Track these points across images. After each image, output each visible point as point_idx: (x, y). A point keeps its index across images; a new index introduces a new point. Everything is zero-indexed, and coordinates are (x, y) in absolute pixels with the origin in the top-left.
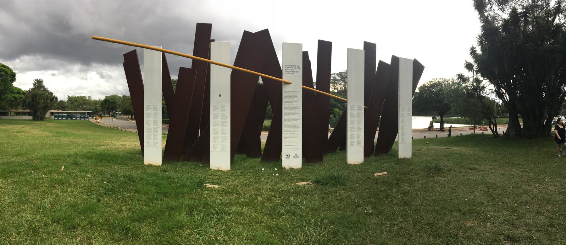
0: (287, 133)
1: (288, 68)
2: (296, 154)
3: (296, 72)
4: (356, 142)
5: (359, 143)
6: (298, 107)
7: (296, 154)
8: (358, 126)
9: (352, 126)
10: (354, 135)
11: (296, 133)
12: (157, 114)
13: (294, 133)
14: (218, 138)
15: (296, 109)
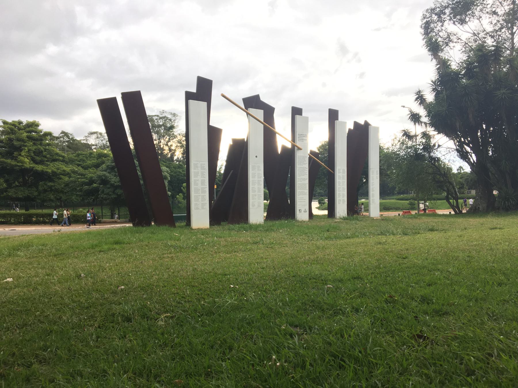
0: (300, 191)
13: (304, 191)
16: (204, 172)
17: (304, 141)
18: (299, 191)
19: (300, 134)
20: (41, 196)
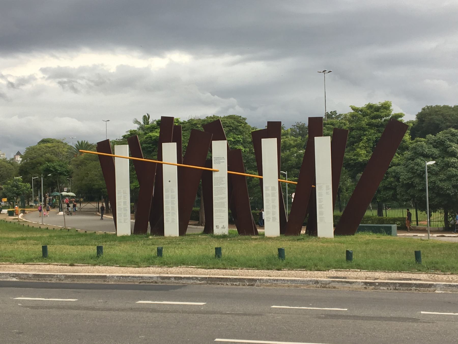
1: (216, 159)
2: (223, 226)
3: (222, 162)
4: (272, 218)
5: (274, 219)
6: (224, 189)
7: (223, 226)
8: (273, 204)
9: (267, 204)
10: (270, 212)
11: (223, 209)
12: (126, 197)
14: (169, 213)
15: (223, 191)
16: (126, 196)
17: (221, 163)
18: (215, 209)
19: (216, 158)
20: (381, 194)
